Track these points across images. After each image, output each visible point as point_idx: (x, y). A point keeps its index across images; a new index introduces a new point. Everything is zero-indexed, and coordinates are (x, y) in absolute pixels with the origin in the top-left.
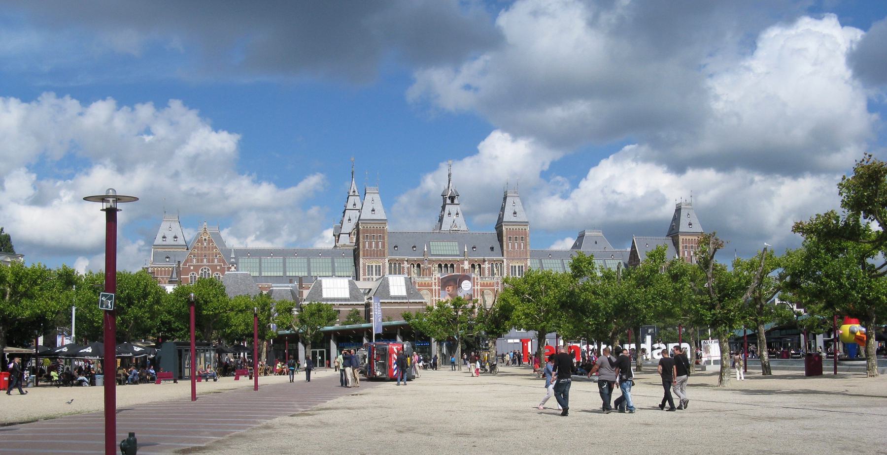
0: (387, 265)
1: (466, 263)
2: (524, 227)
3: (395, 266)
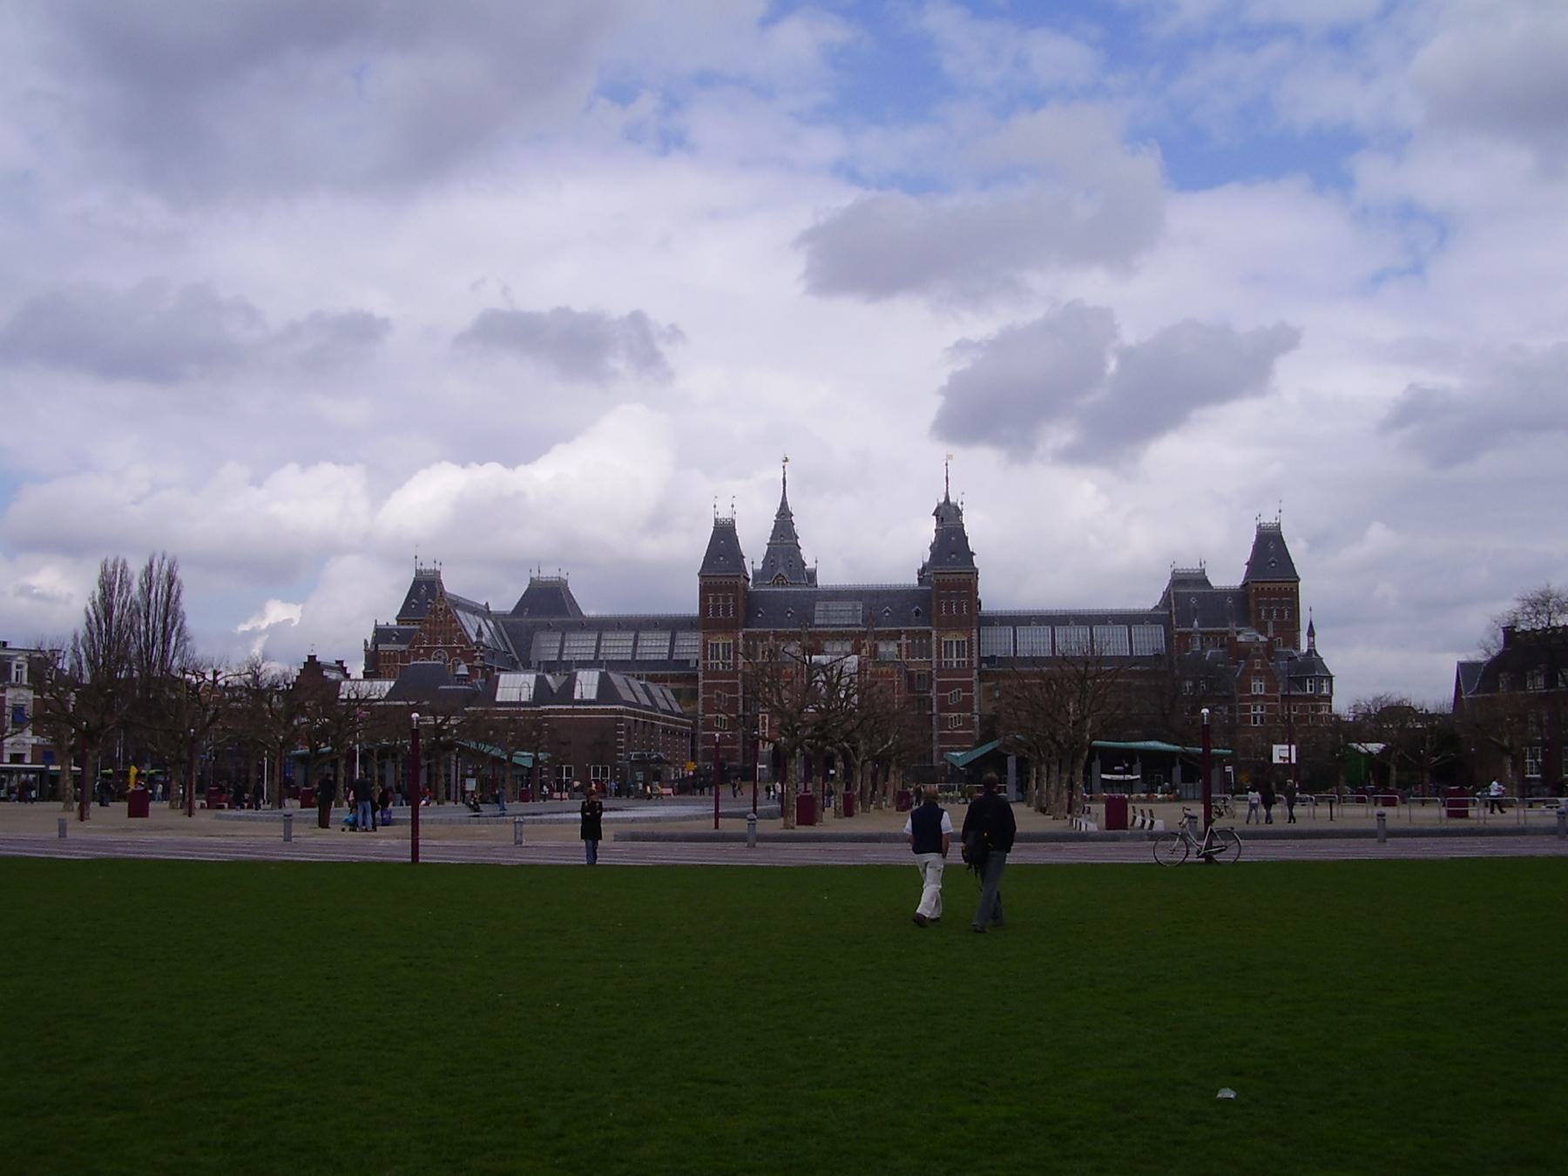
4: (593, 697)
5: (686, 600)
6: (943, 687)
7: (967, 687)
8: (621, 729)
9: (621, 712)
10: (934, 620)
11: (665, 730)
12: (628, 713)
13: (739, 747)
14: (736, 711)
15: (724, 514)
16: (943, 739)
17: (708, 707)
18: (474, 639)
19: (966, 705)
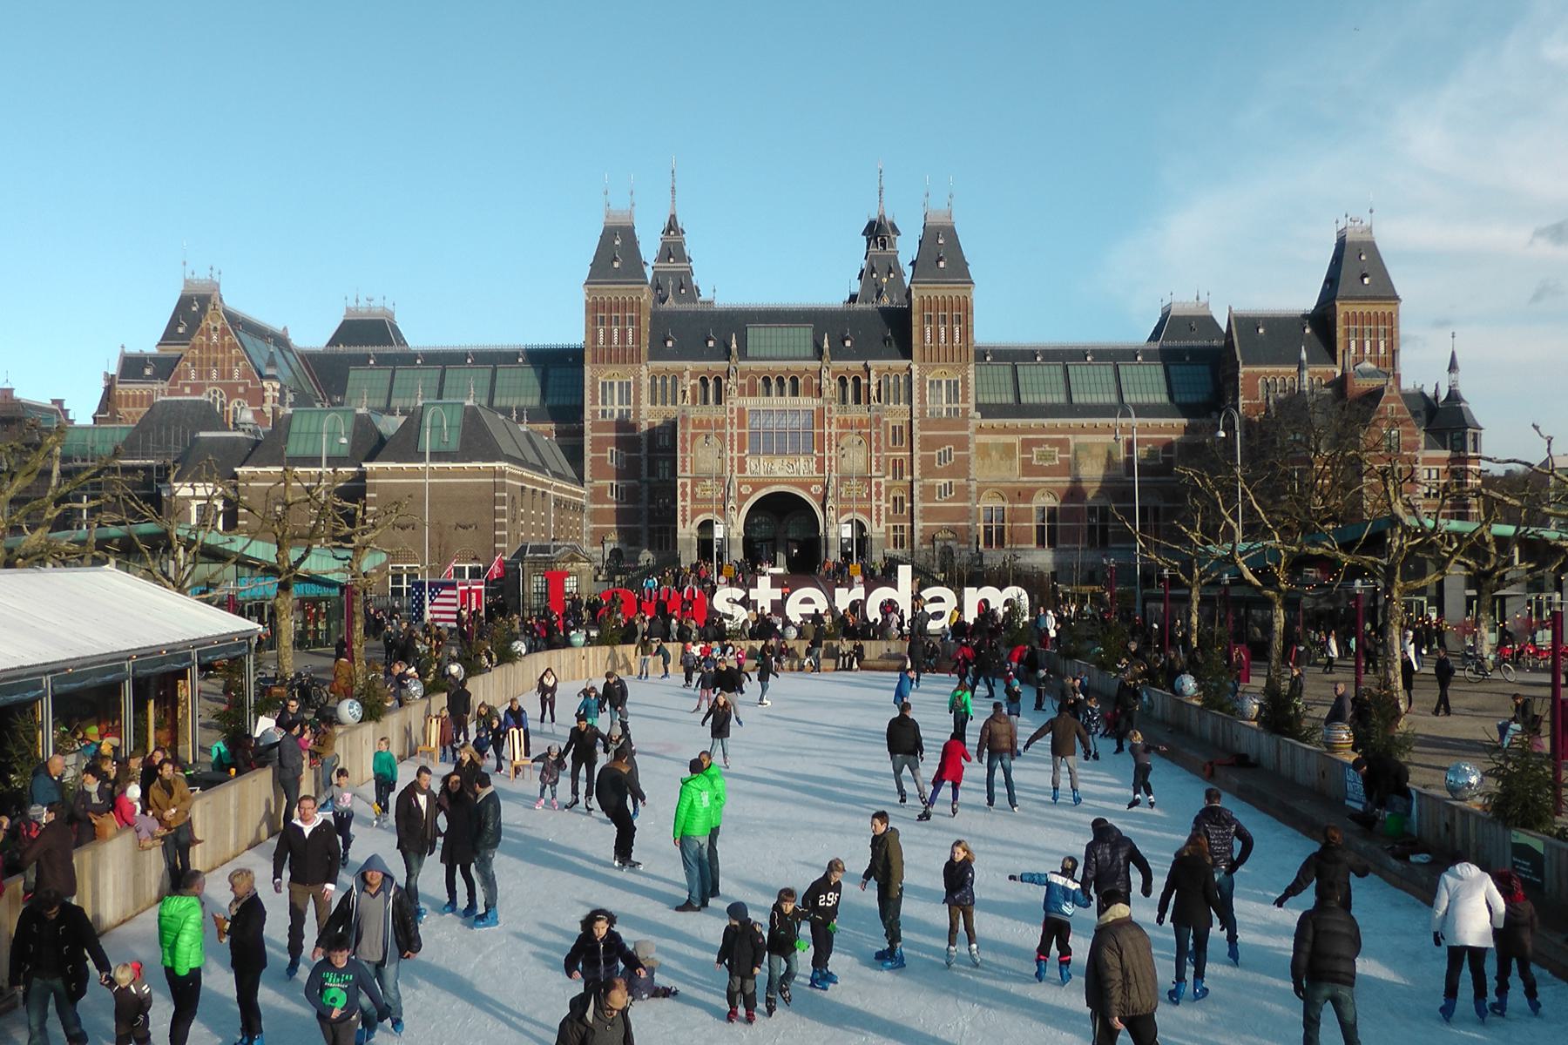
6: (927, 443)
8: (503, 501)
10: (916, 351)
11: (558, 502)
14: (637, 476)
15: (620, 205)
19: (961, 468)
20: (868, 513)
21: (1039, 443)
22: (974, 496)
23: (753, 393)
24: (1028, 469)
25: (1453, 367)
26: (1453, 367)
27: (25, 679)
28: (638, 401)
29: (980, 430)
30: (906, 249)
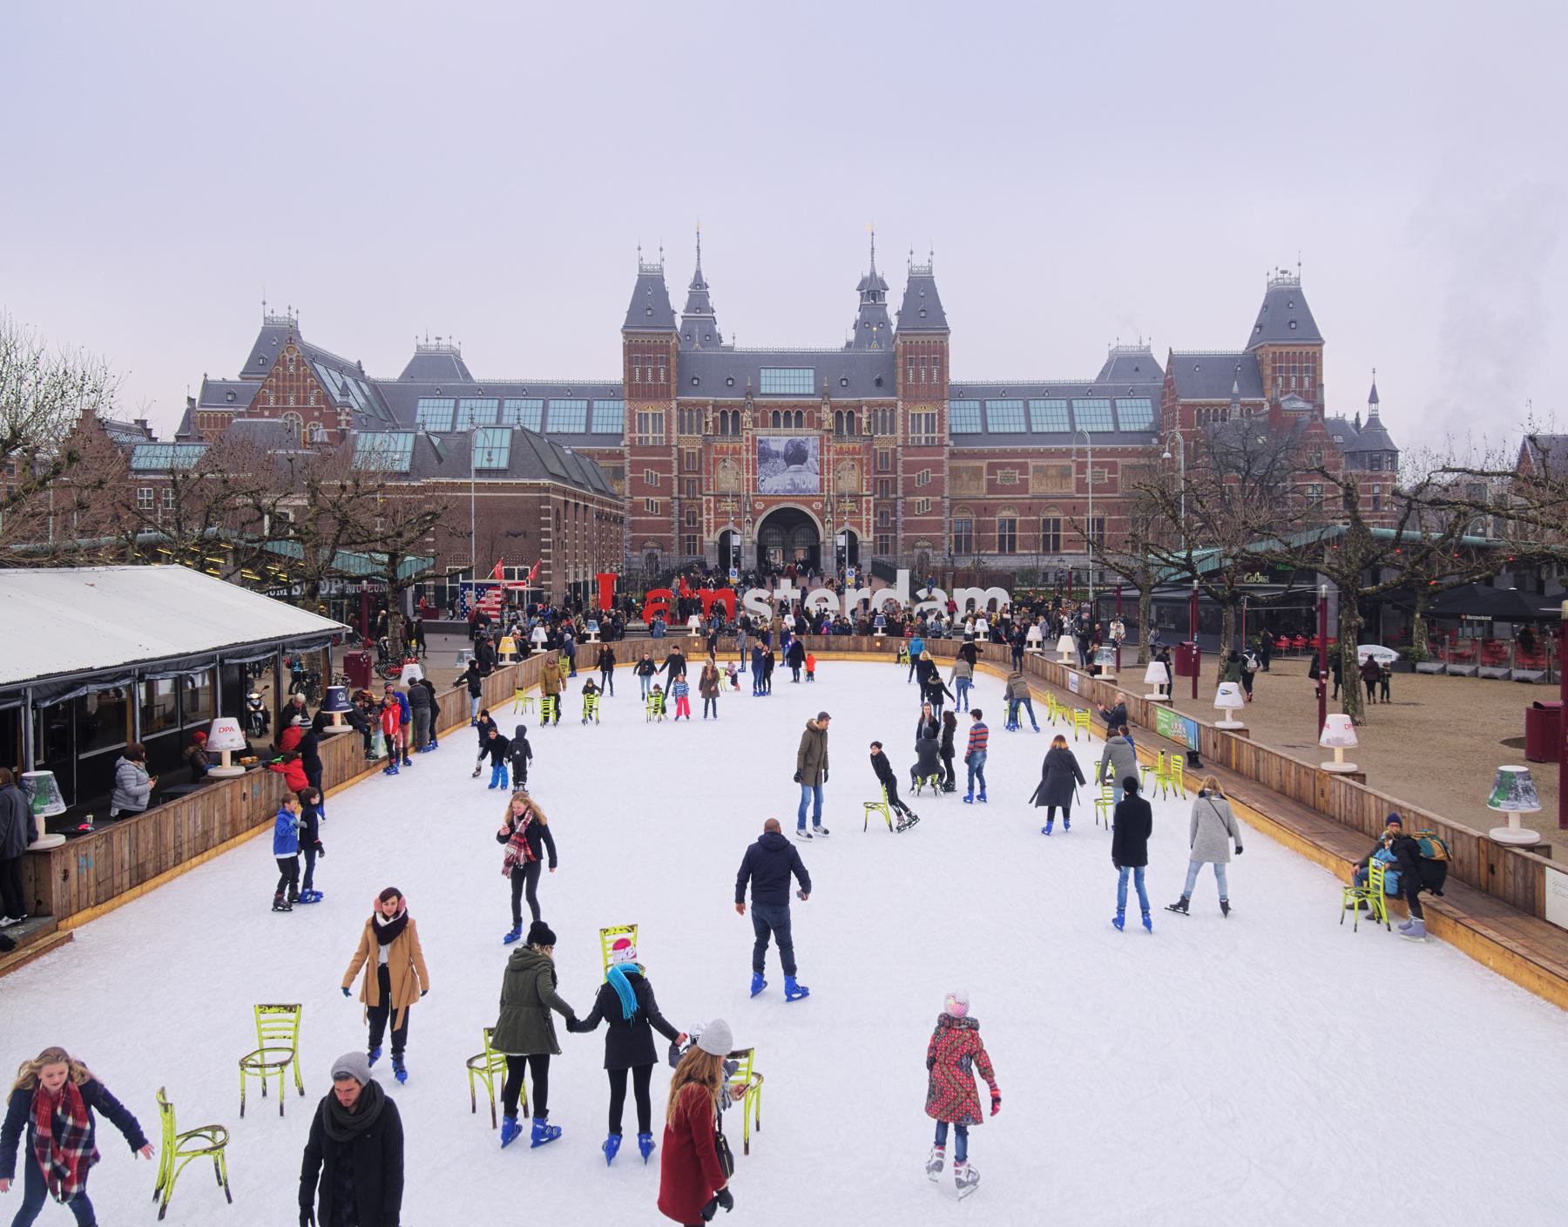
0: (675, 412)
1: (826, 409)
2: (936, 338)
3: (691, 416)
4: (504, 464)
5: (606, 363)
6: (909, 467)
7: (937, 467)
8: (547, 513)
9: (547, 489)
11: (599, 515)
12: (557, 490)
13: (674, 534)
14: (670, 493)
15: (651, 260)
16: (908, 526)
17: (638, 487)
18: (338, 399)
19: (935, 488)
20: (859, 525)
21: (1002, 466)
22: (947, 511)
23: (765, 425)
24: (992, 488)
25: (1374, 399)
26: (1374, 399)
27: (14, 692)
28: (669, 430)
29: (953, 455)
30: (894, 302)
